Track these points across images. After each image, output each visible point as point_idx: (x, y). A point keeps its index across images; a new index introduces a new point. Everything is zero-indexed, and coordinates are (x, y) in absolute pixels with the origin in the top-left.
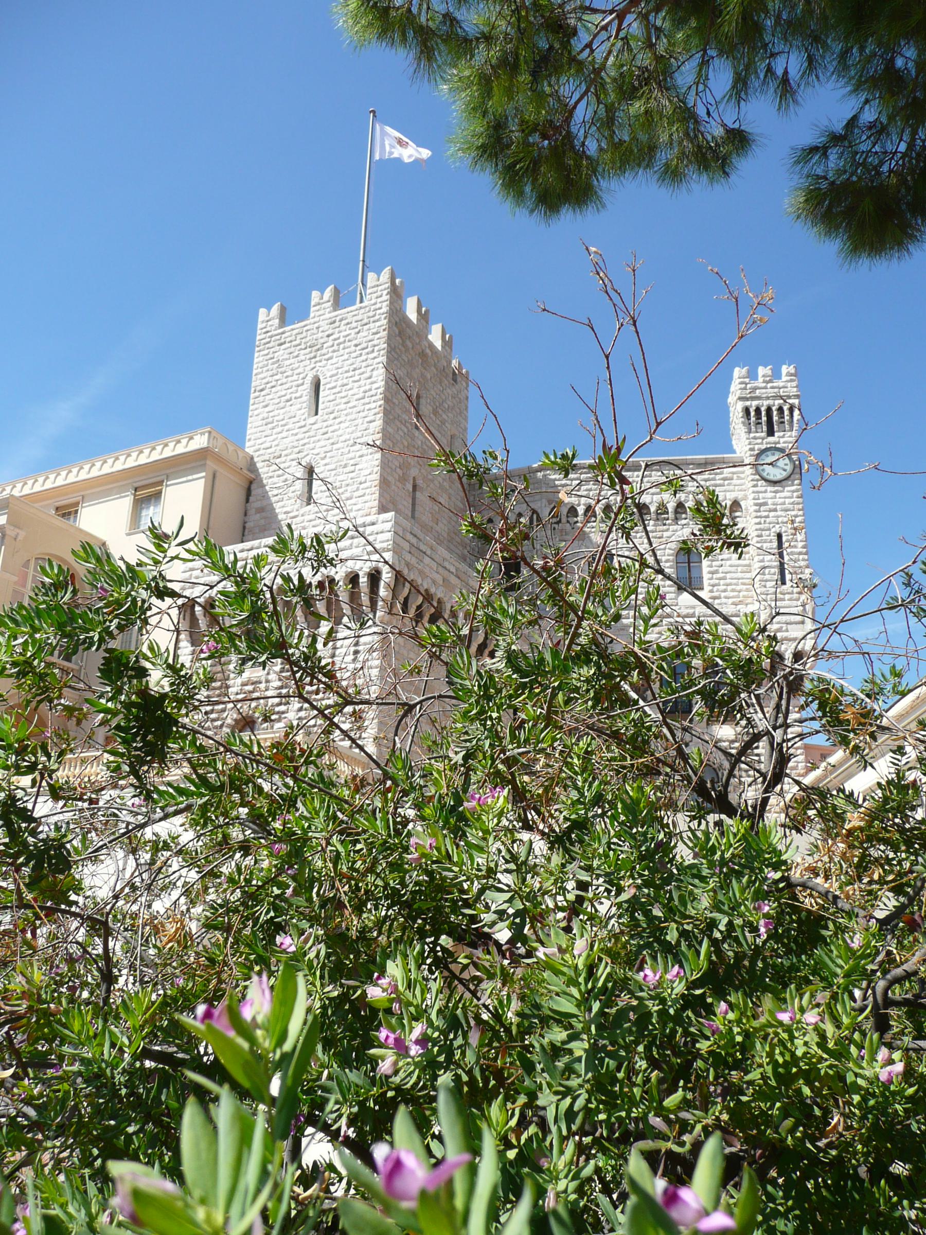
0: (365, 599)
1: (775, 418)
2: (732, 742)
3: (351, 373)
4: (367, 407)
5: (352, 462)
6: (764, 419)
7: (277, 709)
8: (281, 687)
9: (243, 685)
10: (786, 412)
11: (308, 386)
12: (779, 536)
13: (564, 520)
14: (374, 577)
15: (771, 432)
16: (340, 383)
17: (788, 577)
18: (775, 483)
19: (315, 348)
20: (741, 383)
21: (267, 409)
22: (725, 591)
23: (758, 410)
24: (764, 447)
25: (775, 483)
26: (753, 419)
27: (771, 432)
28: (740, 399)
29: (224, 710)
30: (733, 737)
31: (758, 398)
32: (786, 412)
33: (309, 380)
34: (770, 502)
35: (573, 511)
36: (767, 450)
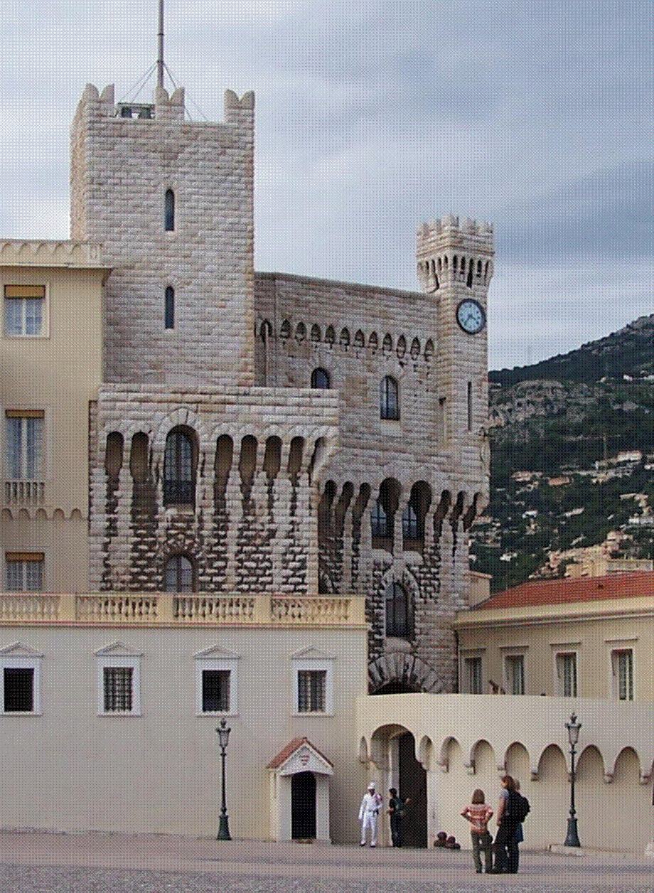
0: (306, 460)
1: (475, 272)
2: (420, 567)
3: (215, 198)
4: (237, 241)
5: (223, 296)
6: (467, 271)
7: (215, 549)
8: (215, 529)
9: (173, 520)
10: (484, 268)
11: (161, 195)
12: (470, 384)
13: (293, 334)
14: (319, 442)
15: (469, 284)
16: (202, 205)
17: (474, 425)
18: (470, 333)
19: (170, 156)
20: (452, 231)
21: (110, 209)
22: (416, 425)
23: (463, 260)
24: (465, 297)
25: (470, 333)
26: (459, 269)
27: (469, 284)
28: (453, 247)
29: (154, 543)
30: (422, 563)
31: (463, 248)
32: (484, 268)
33: (163, 188)
34: (465, 351)
35: (301, 327)
36: (465, 301)
